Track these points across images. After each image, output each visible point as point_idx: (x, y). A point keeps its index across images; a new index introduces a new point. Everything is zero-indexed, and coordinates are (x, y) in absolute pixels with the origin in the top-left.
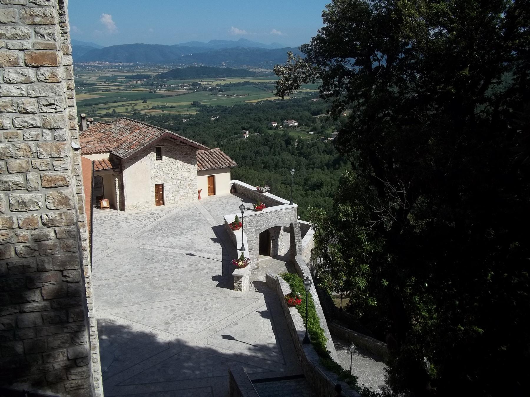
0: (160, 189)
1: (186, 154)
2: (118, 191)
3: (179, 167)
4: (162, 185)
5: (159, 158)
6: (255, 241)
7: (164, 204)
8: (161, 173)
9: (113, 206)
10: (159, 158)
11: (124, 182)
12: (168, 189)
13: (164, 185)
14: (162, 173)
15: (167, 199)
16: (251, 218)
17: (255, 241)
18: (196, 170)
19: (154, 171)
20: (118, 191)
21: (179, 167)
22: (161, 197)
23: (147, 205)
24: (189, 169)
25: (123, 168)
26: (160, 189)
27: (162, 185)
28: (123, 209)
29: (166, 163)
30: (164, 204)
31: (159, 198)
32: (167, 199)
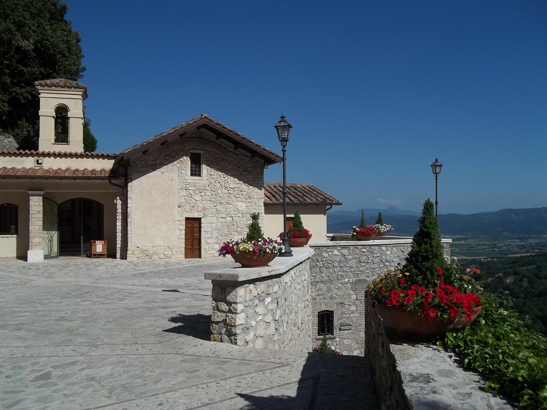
0: (193, 227)
1: (245, 170)
2: (119, 224)
3: (232, 192)
4: (198, 220)
5: (196, 172)
6: (353, 308)
7: (200, 257)
8: (198, 198)
9: (111, 255)
10: (196, 172)
11: (129, 205)
12: (209, 229)
13: (202, 220)
14: (200, 198)
15: (207, 247)
16: (345, 251)
17: (353, 308)
18: (263, 200)
19: (184, 193)
20: (119, 224)
21: (232, 192)
22: (195, 242)
23: (168, 253)
24: (250, 198)
25: (129, 180)
26: (193, 227)
27: (198, 220)
28: (124, 256)
29: (207, 182)
30: (200, 257)
31: (192, 245)
32: (207, 247)
